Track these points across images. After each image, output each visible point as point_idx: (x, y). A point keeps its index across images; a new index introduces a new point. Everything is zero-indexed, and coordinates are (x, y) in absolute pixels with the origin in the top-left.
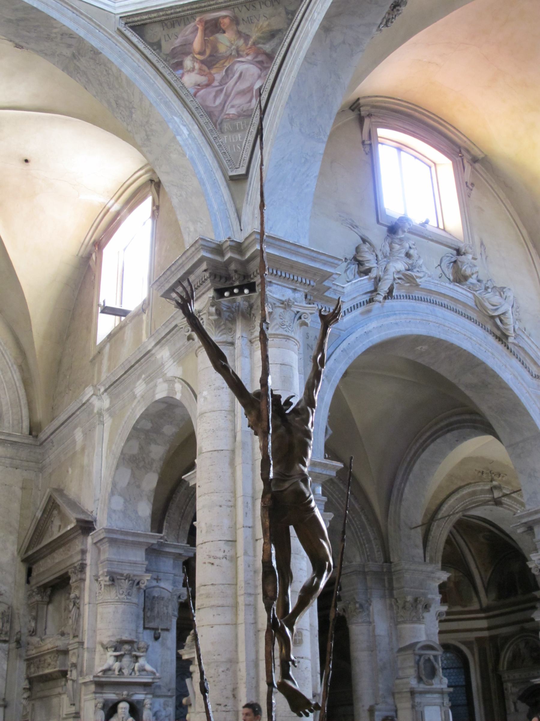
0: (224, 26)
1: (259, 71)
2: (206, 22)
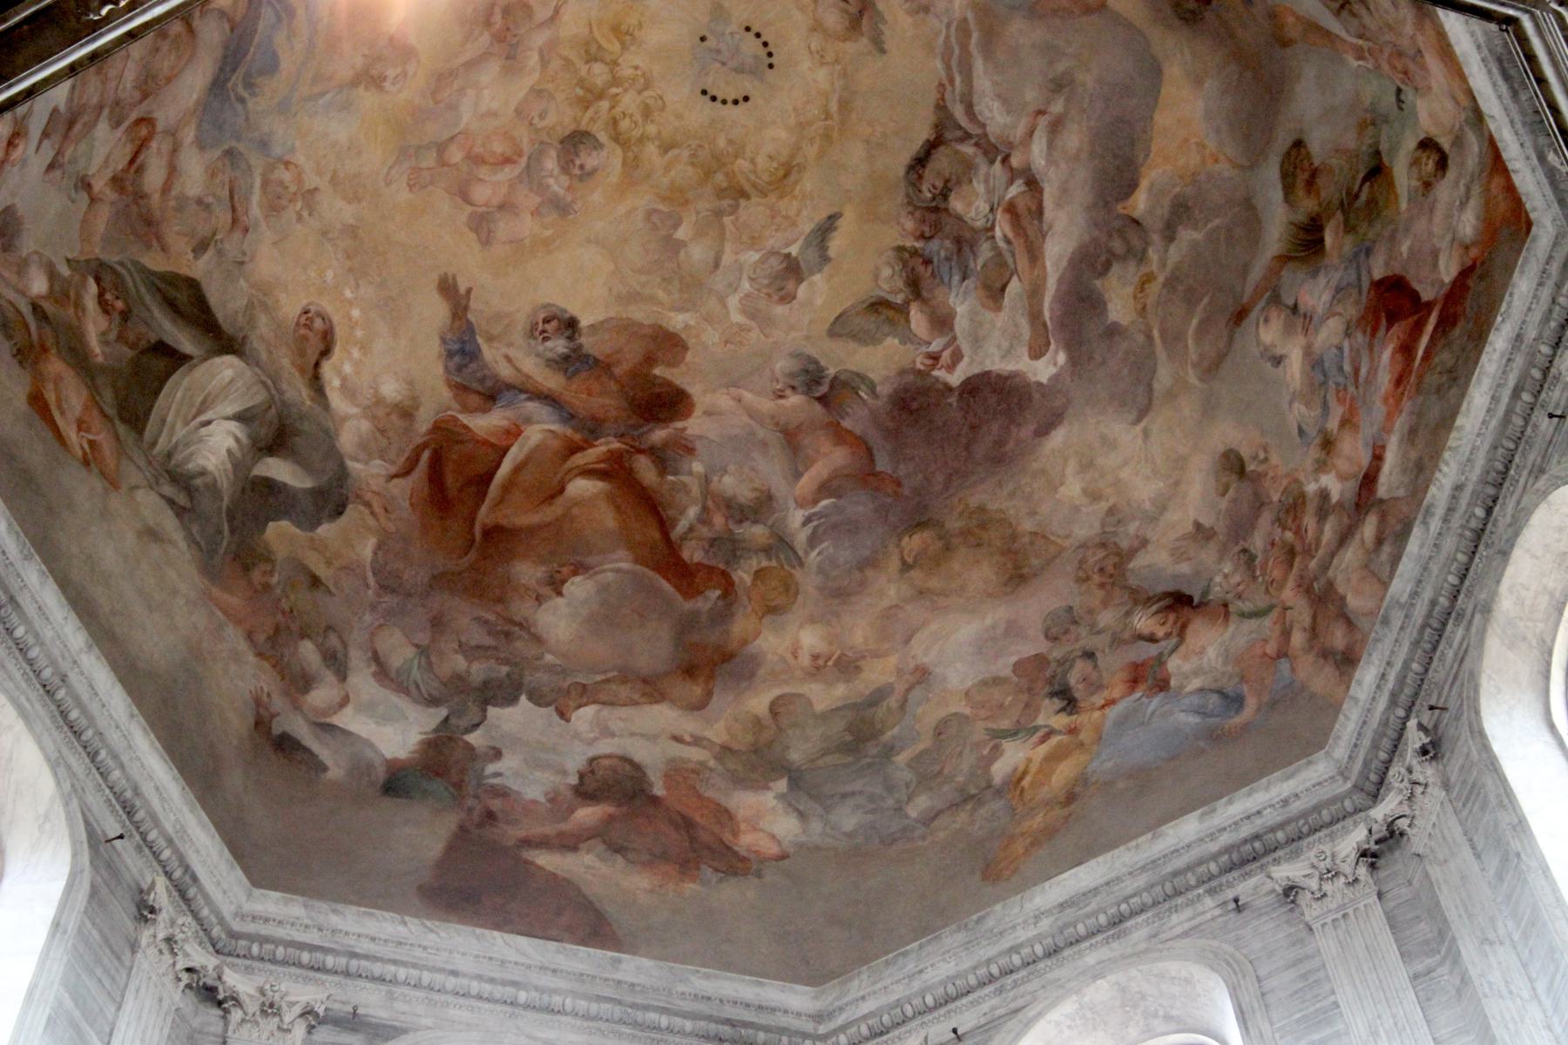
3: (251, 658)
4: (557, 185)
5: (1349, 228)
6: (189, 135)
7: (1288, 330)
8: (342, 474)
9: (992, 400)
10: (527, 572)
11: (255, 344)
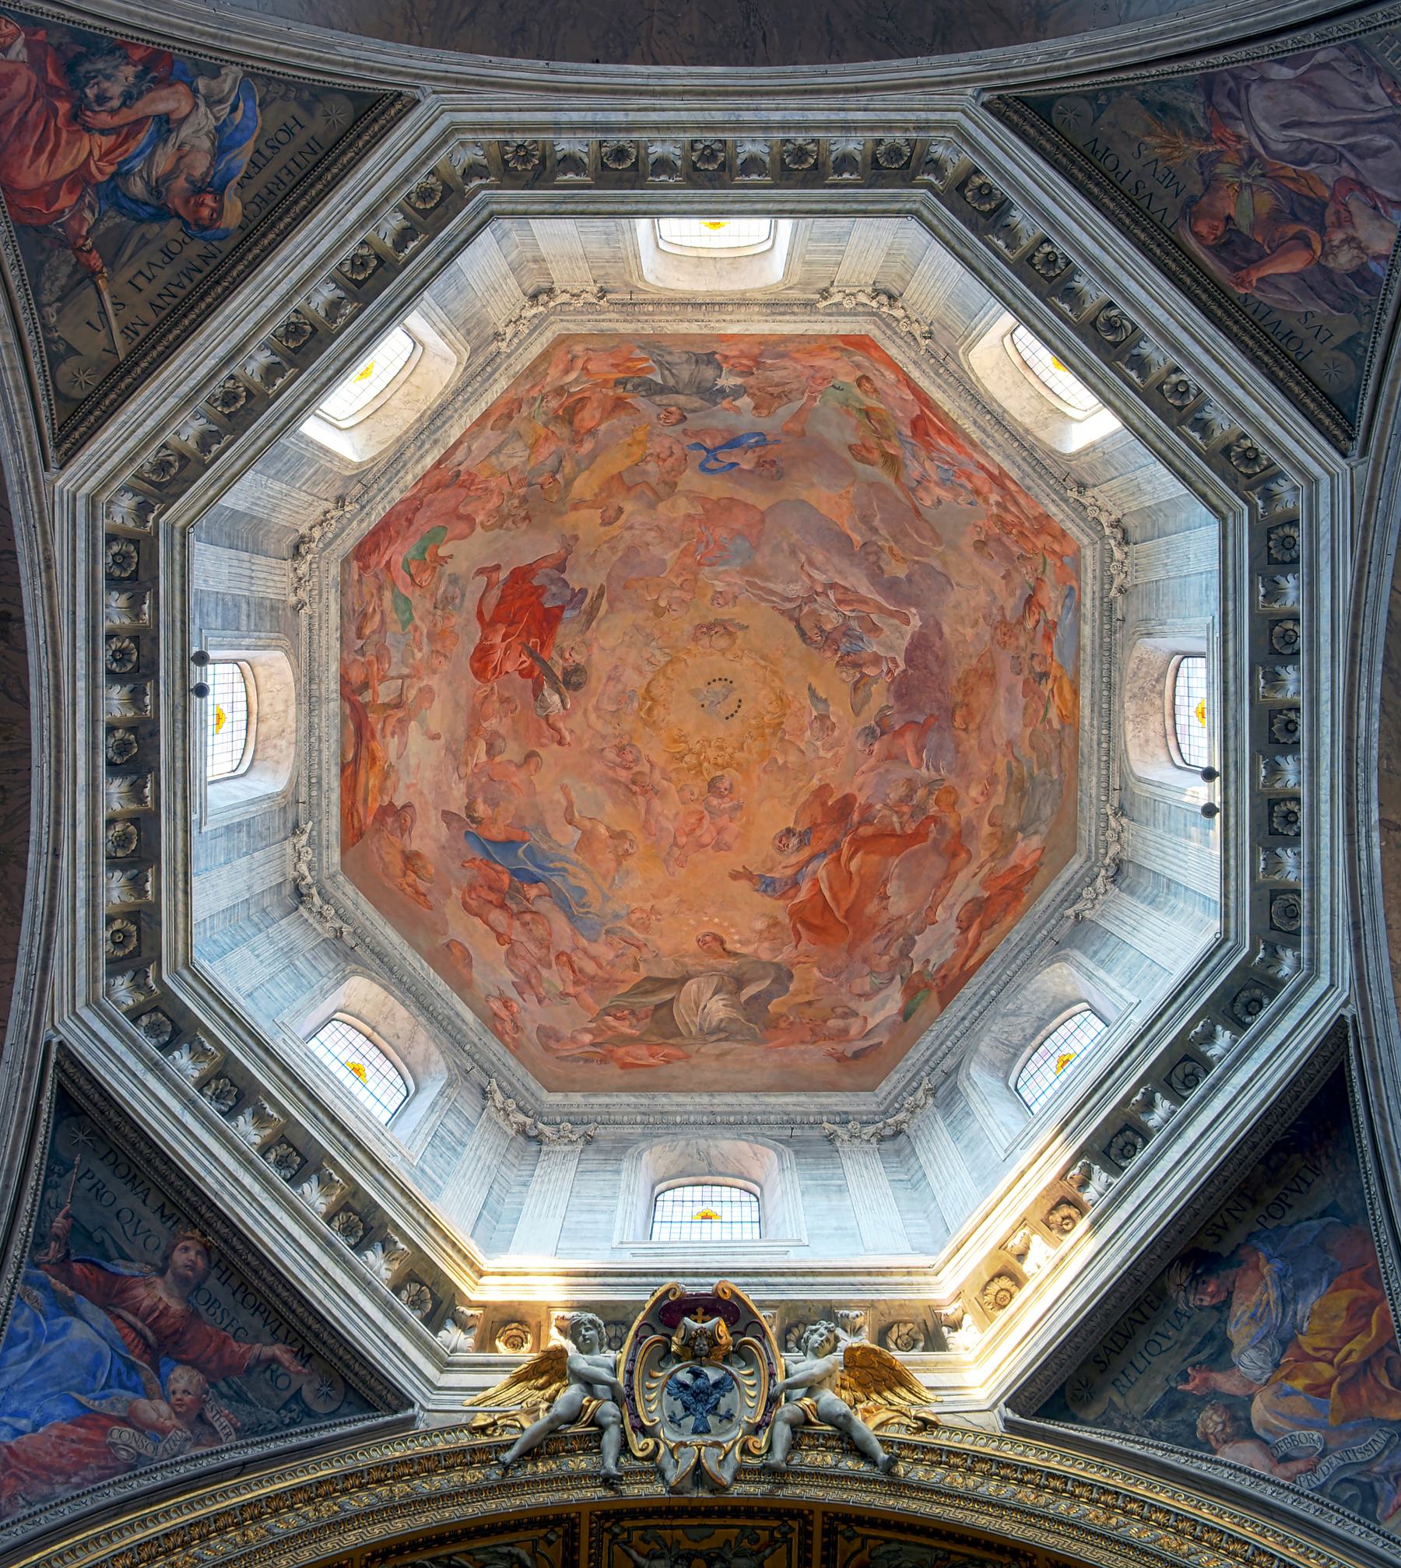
0: (1217, 228)
1: (1253, 87)
2: (1237, 269)
3: (811, 1047)
5: (888, 439)
6: (584, 943)
7: (927, 489)
8: (778, 966)
9: (918, 653)
10: (872, 908)
11: (692, 969)
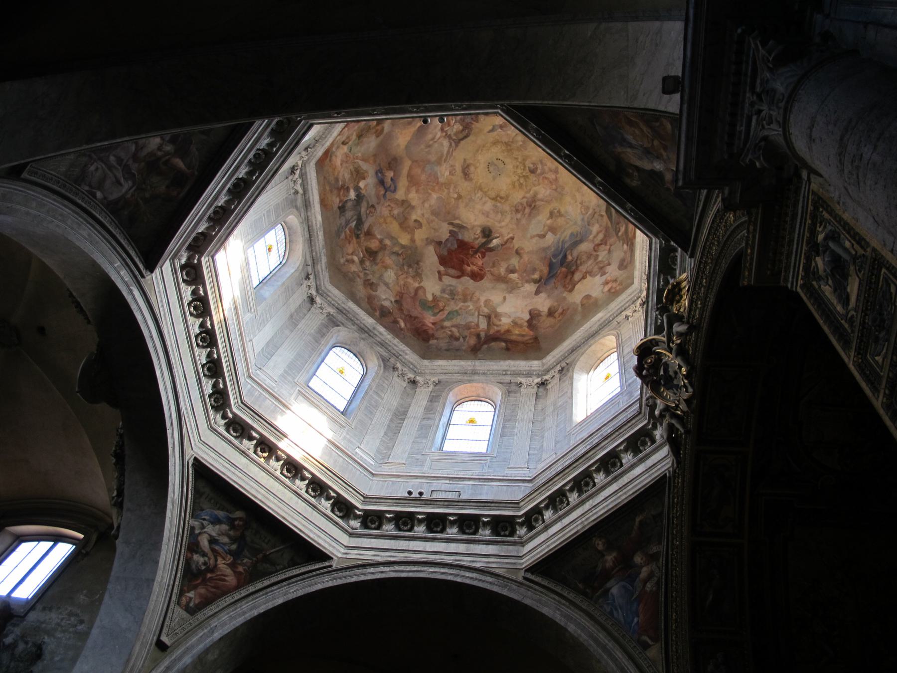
4: (540, 166)
